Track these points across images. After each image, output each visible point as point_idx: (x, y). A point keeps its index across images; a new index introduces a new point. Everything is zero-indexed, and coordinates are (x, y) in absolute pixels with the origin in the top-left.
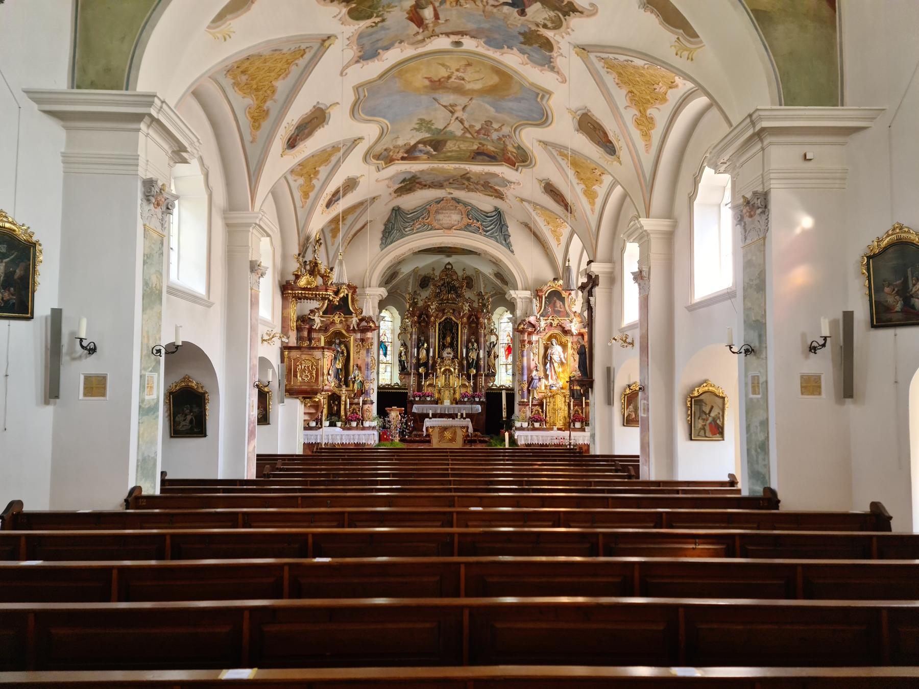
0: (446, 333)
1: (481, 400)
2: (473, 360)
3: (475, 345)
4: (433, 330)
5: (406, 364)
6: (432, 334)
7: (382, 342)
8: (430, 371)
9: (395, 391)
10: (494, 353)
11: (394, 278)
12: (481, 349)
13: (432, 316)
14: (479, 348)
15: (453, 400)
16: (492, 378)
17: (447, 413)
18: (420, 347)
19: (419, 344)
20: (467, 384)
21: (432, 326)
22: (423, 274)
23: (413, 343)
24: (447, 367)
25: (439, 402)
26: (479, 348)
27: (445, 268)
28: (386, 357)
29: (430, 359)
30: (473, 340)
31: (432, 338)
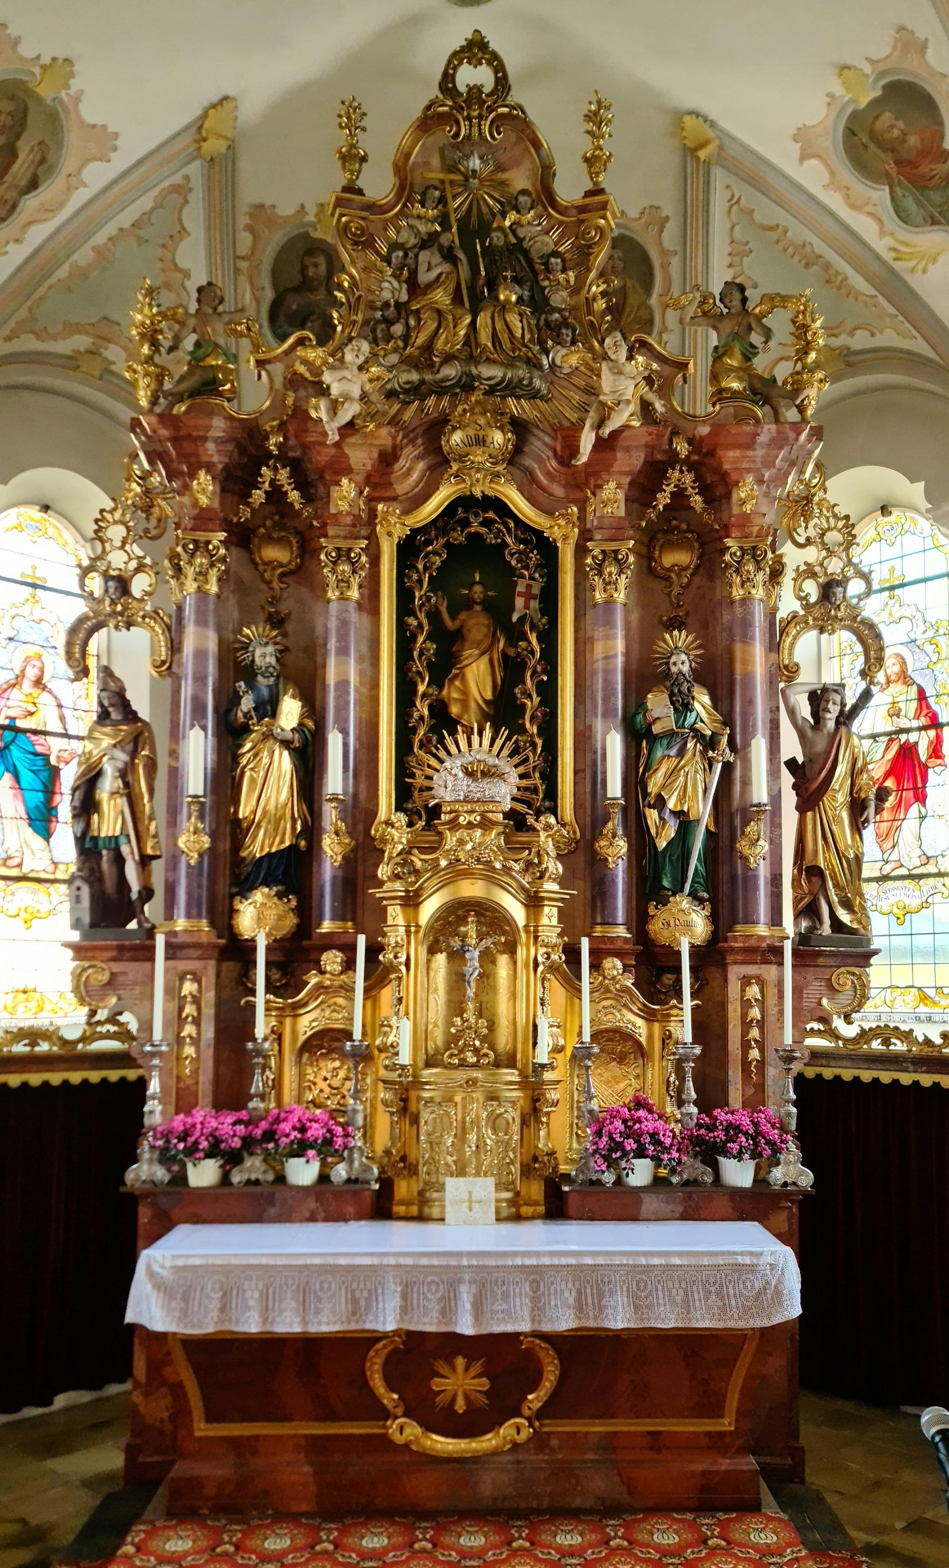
0: (458, 636)
1: (778, 1175)
2: (685, 824)
3: (702, 700)
4: (354, 594)
5: (131, 872)
6: (344, 624)
7: (12, 728)
8: (327, 926)
9: (94, 1076)
10: (854, 773)
11: (33, 184)
12: (748, 734)
13: (341, 467)
14: (728, 721)
15: (527, 1171)
16: (844, 978)
17: (466, 1326)
18: (245, 730)
19: (236, 699)
20: (640, 1027)
21: (343, 554)
22: (286, 209)
23: (187, 690)
24: (472, 889)
25: (403, 1188)
26: (728, 721)
27: (447, 82)
28: (47, 835)
29: (330, 815)
30: (682, 664)
31: (343, 651)
